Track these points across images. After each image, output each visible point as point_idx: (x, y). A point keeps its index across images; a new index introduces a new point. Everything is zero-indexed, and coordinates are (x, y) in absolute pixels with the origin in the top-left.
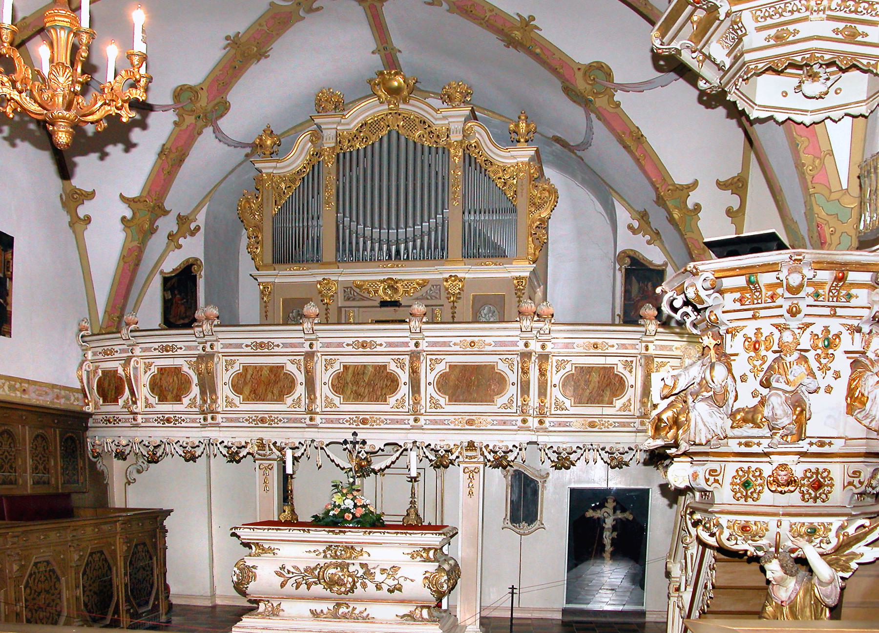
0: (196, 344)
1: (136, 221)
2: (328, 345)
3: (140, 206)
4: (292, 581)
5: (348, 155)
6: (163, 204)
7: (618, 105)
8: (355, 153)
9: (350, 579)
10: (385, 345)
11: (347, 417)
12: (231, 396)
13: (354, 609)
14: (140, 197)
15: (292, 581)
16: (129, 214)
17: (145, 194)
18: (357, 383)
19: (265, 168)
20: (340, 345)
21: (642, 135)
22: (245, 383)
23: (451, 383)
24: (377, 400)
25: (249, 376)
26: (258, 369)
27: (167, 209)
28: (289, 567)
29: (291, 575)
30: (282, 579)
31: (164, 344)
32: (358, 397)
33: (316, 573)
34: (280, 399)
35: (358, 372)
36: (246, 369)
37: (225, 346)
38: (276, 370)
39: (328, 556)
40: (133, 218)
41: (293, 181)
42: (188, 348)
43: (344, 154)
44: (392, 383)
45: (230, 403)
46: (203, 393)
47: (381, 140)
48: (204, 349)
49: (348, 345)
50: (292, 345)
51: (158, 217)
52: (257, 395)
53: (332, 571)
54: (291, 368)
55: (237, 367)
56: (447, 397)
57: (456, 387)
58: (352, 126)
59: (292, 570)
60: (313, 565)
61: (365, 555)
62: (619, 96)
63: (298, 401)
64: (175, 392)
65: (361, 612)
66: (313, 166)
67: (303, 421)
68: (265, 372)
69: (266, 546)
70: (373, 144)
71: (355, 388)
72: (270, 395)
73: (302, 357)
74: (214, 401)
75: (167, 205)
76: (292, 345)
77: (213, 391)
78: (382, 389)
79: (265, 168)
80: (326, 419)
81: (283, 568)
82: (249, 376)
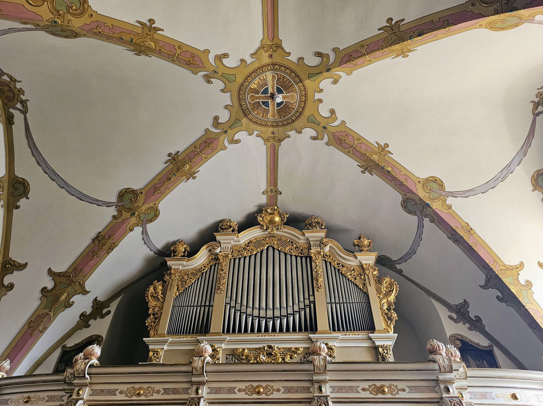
0: (63, 393)
1: (53, 292)
2: (218, 391)
3: (63, 280)
5: (237, 260)
6: (84, 282)
7: (450, 207)
8: (243, 259)
10: (282, 390)
14: (66, 272)
16: (50, 285)
17: (70, 271)
19: (175, 265)
21: (471, 229)
27: (87, 289)
40: (52, 289)
43: (235, 260)
47: (262, 252)
49: (240, 390)
50: (175, 391)
51: (76, 293)
58: (241, 242)
62: (450, 201)
66: (211, 266)
70: (256, 254)
75: (88, 285)
76: (175, 391)
79: (175, 265)
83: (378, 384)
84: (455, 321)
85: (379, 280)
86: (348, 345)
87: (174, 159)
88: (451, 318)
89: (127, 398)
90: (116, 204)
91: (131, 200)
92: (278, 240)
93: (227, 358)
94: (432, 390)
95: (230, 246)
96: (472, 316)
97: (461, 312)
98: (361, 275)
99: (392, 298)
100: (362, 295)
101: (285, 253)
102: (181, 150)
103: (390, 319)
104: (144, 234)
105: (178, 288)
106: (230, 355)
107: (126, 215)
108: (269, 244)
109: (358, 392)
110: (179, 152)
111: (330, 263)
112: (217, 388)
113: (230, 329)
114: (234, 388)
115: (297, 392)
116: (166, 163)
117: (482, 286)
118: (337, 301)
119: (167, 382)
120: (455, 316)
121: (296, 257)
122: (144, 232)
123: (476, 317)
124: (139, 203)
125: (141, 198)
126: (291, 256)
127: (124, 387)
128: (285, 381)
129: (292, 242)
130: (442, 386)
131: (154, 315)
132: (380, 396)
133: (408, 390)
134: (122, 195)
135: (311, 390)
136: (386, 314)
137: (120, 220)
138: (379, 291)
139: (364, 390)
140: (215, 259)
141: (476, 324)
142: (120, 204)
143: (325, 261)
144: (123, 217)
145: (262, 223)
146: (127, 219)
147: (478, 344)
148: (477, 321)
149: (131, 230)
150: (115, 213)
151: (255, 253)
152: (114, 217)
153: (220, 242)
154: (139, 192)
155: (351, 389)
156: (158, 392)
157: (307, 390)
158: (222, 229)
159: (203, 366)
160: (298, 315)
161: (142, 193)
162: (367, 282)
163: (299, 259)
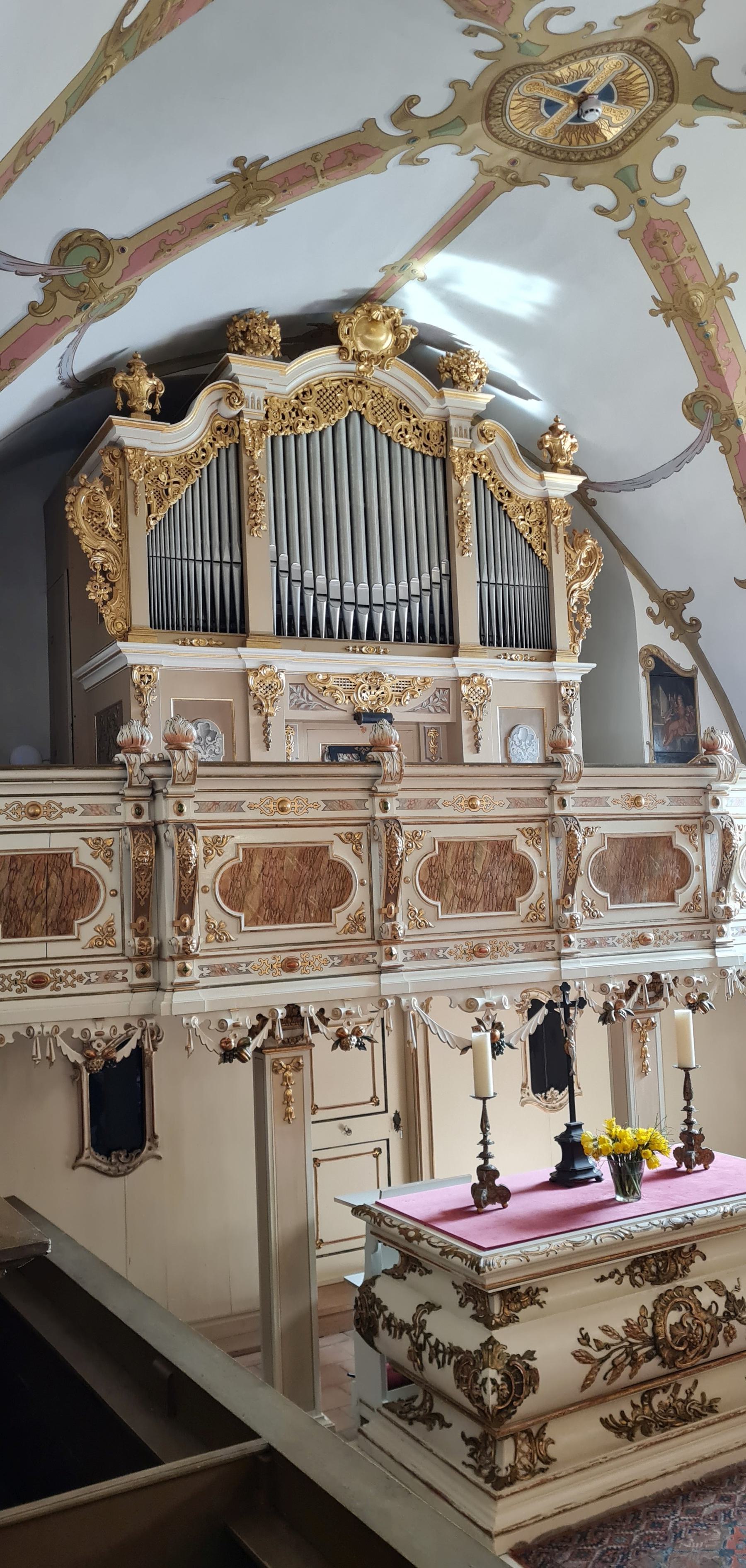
2: (412, 804)
4: (607, 1365)
9: (708, 1328)
11: (451, 945)
12: (217, 916)
13: (677, 1387)
15: (607, 1365)
18: (463, 877)
20: (432, 804)
22: (248, 888)
23: (612, 873)
24: (499, 908)
25: (256, 871)
26: (274, 853)
28: (595, 1334)
29: (603, 1353)
30: (588, 1367)
31: (25, 801)
32: (467, 903)
33: (648, 1331)
34: (324, 914)
35: (465, 852)
36: (250, 852)
37: (203, 807)
38: (313, 855)
39: (638, 1279)
41: (186, 473)
42: (89, 810)
44: (524, 875)
45: (215, 932)
46: (143, 907)
48: (139, 812)
50: (343, 805)
52: (276, 912)
53: (673, 1317)
54: (341, 852)
55: (229, 851)
56: (608, 895)
57: (620, 877)
58: (288, 389)
59: (605, 1339)
60: (634, 1315)
61: (698, 1259)
63: (357, 922)
64: (52, 912)
65: (690, 1393)
67: (370, 959)
68: (290, 861)
69: (522, 1290)
71: (459, 887)
72: (301, 907)
73: (363, 829)
74: (185, 931)
76: (343, 805)
77: (186, 906)
78: (506, 886)
80: (413, 951)
81: (585, 1339)
82: (256, 871)
83: (634, 793)
84: (656, 619)
85: (573, 540)
86: (510, 675)
87: (244, 176)
88: (650, 612)
89: (264, 817)
90: (45, 270)
91: (89, 265)
92: (374, 395)
93: (292, 692)
94: (695, 801)
95: (260, 395)
96: (686, 616)
97: (671, 607)
98: (541, 523)
99: (587, 583)
100: (538, 569)
101: (389, 439)
102: (273, 158)
103: (578, 626)
104: (71, 346)
105: (149, 506)
106: (297, 685)
107: (65, 305)
108: (355, 404)
109: (608, 805)
110: (267, 158)
111: (485, 482)
112: (409, 800)
113: (291, 627)
114: (436, 801)
115: (527, 806)
116: (217, 181)
117: (740, 581)
118: (493, 580)
119: (329, 790)
120: (656, 609)
121: (413, 451)
122: (74, 344)
123: (692, 619)
124: (106, 280)
125: (119, 262)
126: (402, 447)
127: (254, 798)
128: (513, 789)
129: (406, 409)
130: (710, 797)
131: (104, 573)
132: (634, 810)
133: (668, 801)
134: (69, 245)
135: (547, 802)
136: (574, 615)
137: (47, 320)
138: (569, 566)
139: (615, 802)
140: (226, 429)
141: (689, 632)
142: (55, 273)
143: (475, 475)
144: (57, 313)
145: (345, 341)
146: (67, 318)
147: (677, 666)
148: (691, 625)
149: (57, 342)
150: (37, 296)
151: (321, 428)
152: (33, 308)
153: (237, 381)
154: (116, 246)
155: (598, 801)
156: (316, 806)
157: (540, 802)
158: (249, 344)
159: (402, 770)
160: (418, 604)
161: (123, 250)
162: (553, 543)
163: (419, 459)
